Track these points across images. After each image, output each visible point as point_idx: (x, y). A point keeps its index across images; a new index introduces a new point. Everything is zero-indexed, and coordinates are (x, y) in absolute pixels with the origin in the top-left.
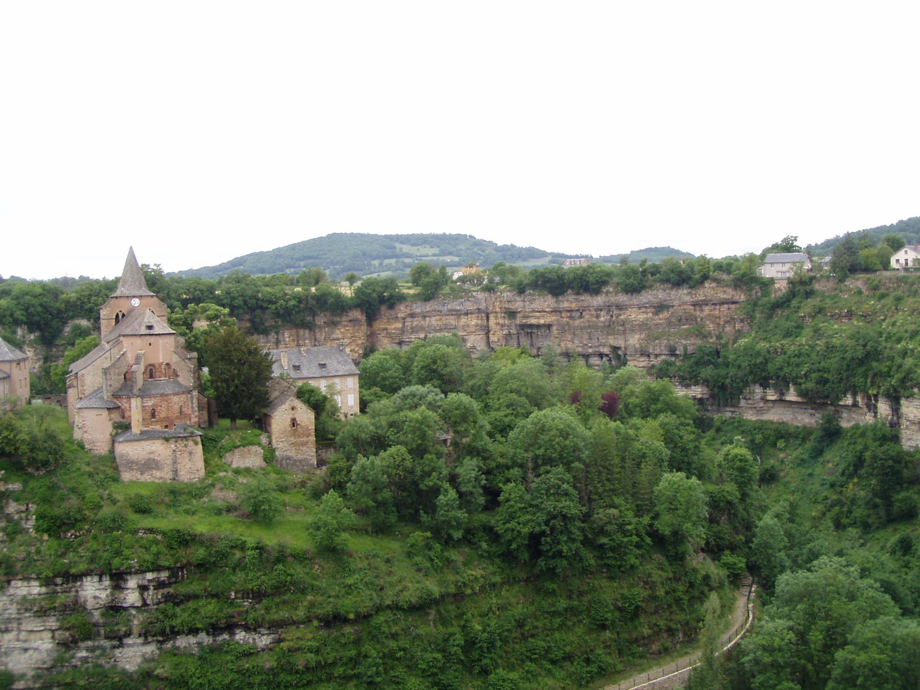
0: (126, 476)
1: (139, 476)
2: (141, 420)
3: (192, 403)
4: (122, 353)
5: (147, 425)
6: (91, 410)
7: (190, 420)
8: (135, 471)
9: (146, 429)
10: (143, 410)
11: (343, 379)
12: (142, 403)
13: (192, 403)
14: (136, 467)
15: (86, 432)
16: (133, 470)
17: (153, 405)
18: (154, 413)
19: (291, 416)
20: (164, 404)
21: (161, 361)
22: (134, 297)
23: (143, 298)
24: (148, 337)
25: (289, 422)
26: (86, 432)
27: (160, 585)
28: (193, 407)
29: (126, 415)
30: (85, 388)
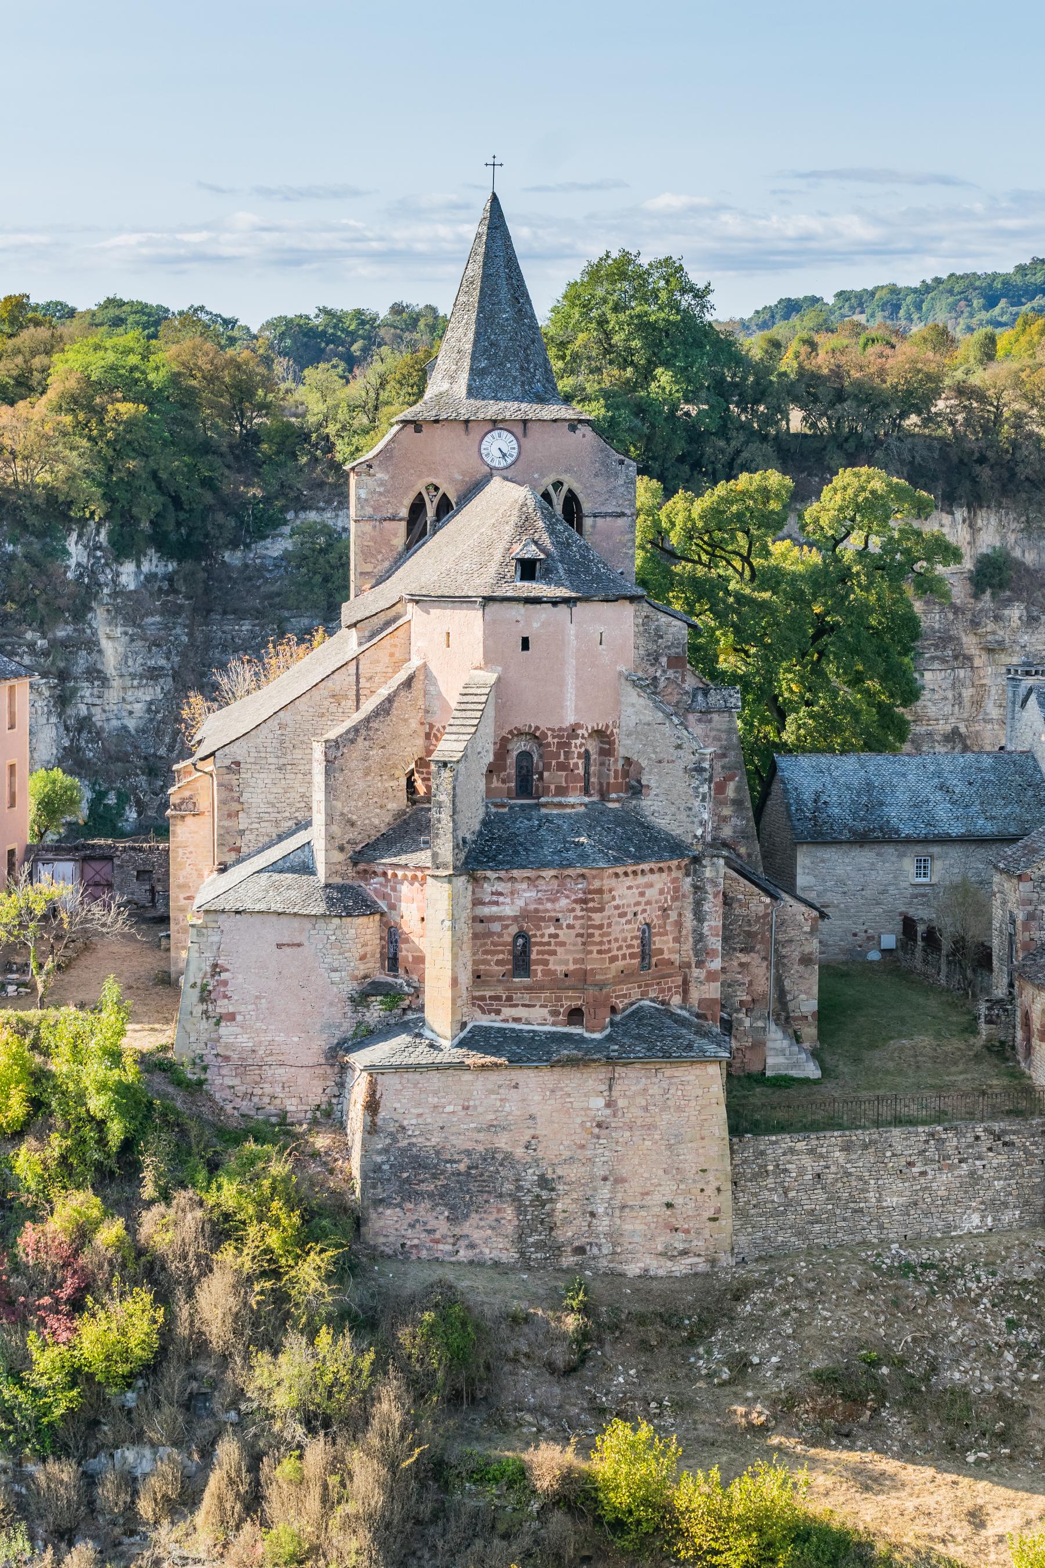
1: (442, 1227)
2: (465, 978)
3: (699, 916)
4: (402, 676)
6: (257, 919)
7: (685, 992)
8: (427, 1204)
9: (485, 1021)
10: (476, 936)
12: (477, 902)
13: (699, 916)
14: (424, 1187)
15: (232, 1017)
16: (419, 1195)
17: (525, 915)
18: (525, 951)
26: (232, 1017)
28: (699, 938)
29: (405, 953)
30: (243, 821)
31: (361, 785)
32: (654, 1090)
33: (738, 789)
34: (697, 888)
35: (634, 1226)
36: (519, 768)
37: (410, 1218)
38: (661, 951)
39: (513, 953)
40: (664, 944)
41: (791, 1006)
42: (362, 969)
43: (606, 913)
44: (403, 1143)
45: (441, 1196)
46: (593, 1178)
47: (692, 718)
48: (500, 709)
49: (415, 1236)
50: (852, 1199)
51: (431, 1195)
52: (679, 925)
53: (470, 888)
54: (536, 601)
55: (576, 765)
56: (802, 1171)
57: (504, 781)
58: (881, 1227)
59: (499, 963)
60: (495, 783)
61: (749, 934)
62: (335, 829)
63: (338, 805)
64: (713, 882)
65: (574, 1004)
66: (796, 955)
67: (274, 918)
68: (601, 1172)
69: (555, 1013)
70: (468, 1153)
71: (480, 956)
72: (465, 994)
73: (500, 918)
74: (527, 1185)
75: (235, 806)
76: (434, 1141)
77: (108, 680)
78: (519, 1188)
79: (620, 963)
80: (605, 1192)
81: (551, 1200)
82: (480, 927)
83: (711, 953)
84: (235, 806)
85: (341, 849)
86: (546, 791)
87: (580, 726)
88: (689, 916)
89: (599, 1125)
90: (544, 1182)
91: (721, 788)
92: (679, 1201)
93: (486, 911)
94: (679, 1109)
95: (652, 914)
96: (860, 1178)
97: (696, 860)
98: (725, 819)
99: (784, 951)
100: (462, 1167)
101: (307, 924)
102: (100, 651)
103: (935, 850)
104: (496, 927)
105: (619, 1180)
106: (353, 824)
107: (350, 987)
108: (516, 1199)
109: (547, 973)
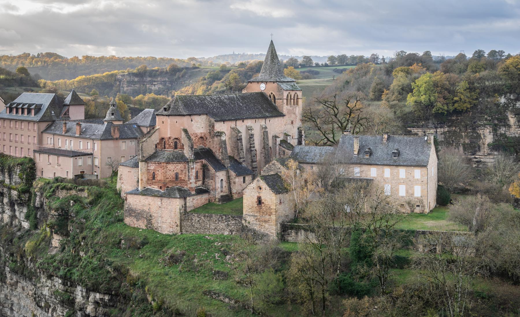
0: (128, 220)
1: (135, 222)
3: (189, 172)
5: (150, 184)
8: (133, 218)
9: (149, 187)
10: (148, 172)
11: (410, 169)
12: (148, 167)
13: (189, 172)
14: (133, 215)
15: (123, 183)
16: (132, 216)
17: (154, 170)
19: (258, 194)
21: (169, 136)
22: (262, 82)
23: (268, 84)
24: (162, 117)
25: (255, 199)
26: (123, 183)
28: (189, 176)
32: (168, 202)
33: (222, 150)
34: (188, 167)
35: (164, 226)
37: (131, 219)
45: (135, 216)
46: (158, 216)
49: (132, 223)
50: (204, 226)
51: (134, 216)
52: (186, 173)
53: (147, 164)
58: (209, 232)
61: (212, 177)
66: (233, 182)
69: (158, 187)
70: (140, 210)
72: (145, 182)
77: (511, 126)
79: (170, 179)
80: (160, 219)
88: (187, 172)
90: (151, 216)
91: (219, 150)
92: (171, 222)
93: (149, 168)
94: (172, 206)
95: (179, 172)
97: (188, 162)
98: (220, 155)
99: (231, 181)
102: (509, 120)
103: (313, 165)
104: (150, 171)
105: (162, 217)
109: (157, 180)
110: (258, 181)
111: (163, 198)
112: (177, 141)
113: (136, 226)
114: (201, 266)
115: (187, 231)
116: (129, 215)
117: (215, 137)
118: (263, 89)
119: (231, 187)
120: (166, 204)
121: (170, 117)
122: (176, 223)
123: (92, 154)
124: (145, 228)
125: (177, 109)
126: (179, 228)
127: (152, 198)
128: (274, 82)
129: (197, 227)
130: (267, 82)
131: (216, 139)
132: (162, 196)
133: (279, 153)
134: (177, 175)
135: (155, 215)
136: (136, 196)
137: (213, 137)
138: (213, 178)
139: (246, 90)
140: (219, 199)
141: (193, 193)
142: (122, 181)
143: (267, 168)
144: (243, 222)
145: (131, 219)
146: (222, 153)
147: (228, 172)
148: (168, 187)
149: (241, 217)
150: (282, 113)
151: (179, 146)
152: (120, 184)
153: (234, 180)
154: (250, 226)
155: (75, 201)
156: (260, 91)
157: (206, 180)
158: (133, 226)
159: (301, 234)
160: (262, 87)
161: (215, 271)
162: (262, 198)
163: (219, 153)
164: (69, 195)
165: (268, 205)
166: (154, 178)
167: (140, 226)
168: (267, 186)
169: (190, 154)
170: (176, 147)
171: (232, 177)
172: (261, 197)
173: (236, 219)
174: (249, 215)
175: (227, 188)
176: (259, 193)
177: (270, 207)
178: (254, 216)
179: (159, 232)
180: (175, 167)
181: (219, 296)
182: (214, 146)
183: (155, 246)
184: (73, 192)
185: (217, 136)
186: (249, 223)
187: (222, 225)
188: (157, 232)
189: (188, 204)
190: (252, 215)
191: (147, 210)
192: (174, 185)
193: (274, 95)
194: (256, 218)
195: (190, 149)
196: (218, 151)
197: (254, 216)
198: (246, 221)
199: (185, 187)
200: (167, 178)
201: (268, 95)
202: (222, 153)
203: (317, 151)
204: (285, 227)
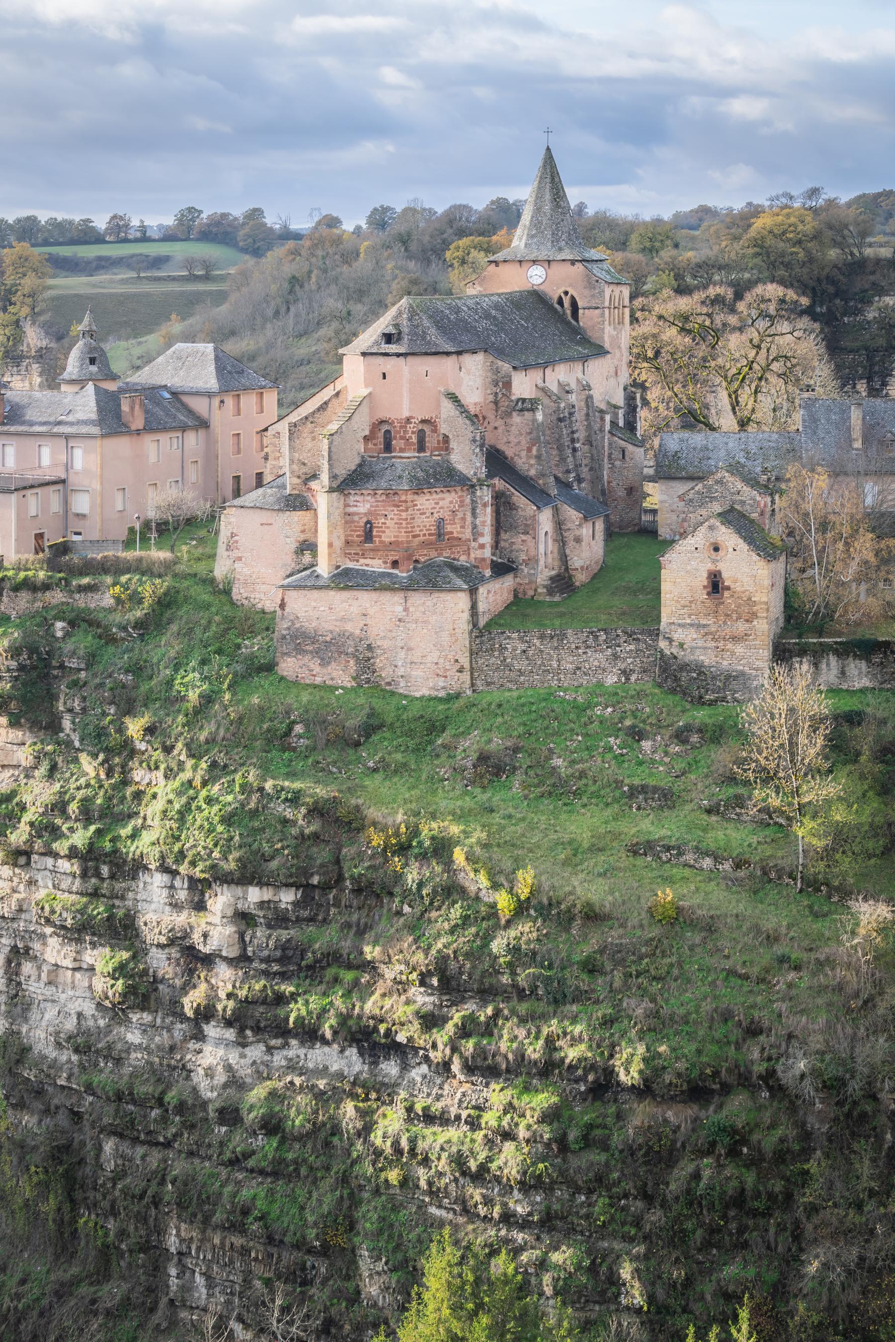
0: (289, 666)
1: (317, 669)
3: (474, 515)
5: (355, 557)
6: (251, 511)
8: (309, 657)
9: (351, 565)
10: (346, 522)
12: (346, 505)
13: (474, 515)
14: (310, 648)
15: (240, 559)
16: (306, 651)
17: (369, 513)
18: (371, 531)
19: (710, 566)
20: (393, 514)
21: (406, 414)
22: (534, 262)
25: (702, 579)
26: (240, 559)
27: (279, 919)
28: (475, 527)
31: (310, 445)
32: (429, 603)
33: (538, 450)
35: (417, 673)
36: (385, 438)
37: (301, 663)
38: (452, 533)
39: (365, 531)
40: (453, 529)
41: (570, 563)
42: (302, 537)
43: (410, 512)
44: (297, 626)
45: (317, 653)
46: (396, 647)
47: (514, 414)
48: (372, 409)
50: (543, 664)
51: (311, 652)
52: (463, 519)
53: (342, 498)
54: (386, 355)
55: (411, 438)
56: (515, 650)
57: (375, 445)
58: (559, 680)
59: (358, 536)
60: (370, 446)
61: (526, 525)
62: (295, 467)
63: (297, 455)
64: (480, 497)
65: (395, 558)
66: (572, 537)
67: (259, 511)
68: (401, 644)
69: (385, 563)
70: (331, 632)
71: (349, 533)
72: (339, 551)
73: (358, 514)
74: (361, 649)
75: (278, 454)
76: (314, 625)
78: (357, 650)
79: (422, 538)
80: (402, 654)
81: (373, 658)
82: (348, 518)
83: (482, 535)
84: (278, 454)
85: (299, 477)
86: (395, 451)
87: (413, 418)
89: (400, 620)
90: (370, 648)
91: (529, 450)
94: (442, 614)
95: (447, 515)
96: (549, 654)
97: (473, 486)
98: (532, 465)
99: (565, 534)
100: (328, 639)
101: (274, 514)
104: (356, 518)
106: (304, 464)
107: (294, 546)
108: (354, 656)
109: (381, 542)
110: (711, 528)
111: (410, 593)
112: (427, 428)
113: (318, 680)
114: (580, 778)
115: (488, 684)
116: (296, 649)
117: (514, 414)
118: (536, 281)
119: (568, 551)
120: (421, 609)
121: (409, 358)
122: (457, 661)
123: (63, 482)
124: (349, 683)
125: (424, 338)
126: (466, 677)
127: (374, 595)
128: (573, 262)
129: (520, 671)
130: (549, 261)
131: (516, 419)
132: (408, 587)
133: (610, 455)
134: (440, 523)
135: (386, 644)
136: (316, 594)
137: (508, 414)
138: (530, 528)
139: (481, 285)
140: (545, 587)
141: (488, 573)
142: (236, 553)
143: (698, 493)
144: (663, 644)
145: (301, 663)
146: (538, 457)
147: (556, 511)
148: (417, 561)
149: (655, 634)
150: (602, 347)
151: (431, 441)
152: (229, 562)
153: (577, 533)
154: (685, 656)
155: (72, 624)
156: (528, 287)
157: (504, 536)
158: (308, 682)
159: (828, 665)
160: (536, 276)
161: (631, 787)
162: (725, 575)
163: (529, 457)
164: (38, 605)
165: (744, 592)
166: (368, 536)
167: (332, 679)
168: (741, 541)
169: (478, 465)
170: (421, 447)
171: (569, 525)
172: (720, 572)
173: (638, 640)
174: (679, 625)
175: (556, 554)
176: (714, 561)
177: (749, 599)
178: (699, 626)
179: (401, 691)
180: (437, 503)
181: (680, 854)
182: (512, 438)
183: (410, 734)
184: (57, 597)
185: (521, 410)
186: (681, 645)
187: (597, 659)
188: (393, 693)
189: (482, 607)
190: (691, 625)
191: (358, 632)
192: (433, 554)
193: (573, 299)
194: (706, 630)
195: (478, 450)
196: (524, 453)
197: (699, 626)
198: (670, 640)
199: (463, 558)
200: (414, 536)
201: (556, 298)
202: (538, 457)
203: (731, 445)
204: (784, 651)
